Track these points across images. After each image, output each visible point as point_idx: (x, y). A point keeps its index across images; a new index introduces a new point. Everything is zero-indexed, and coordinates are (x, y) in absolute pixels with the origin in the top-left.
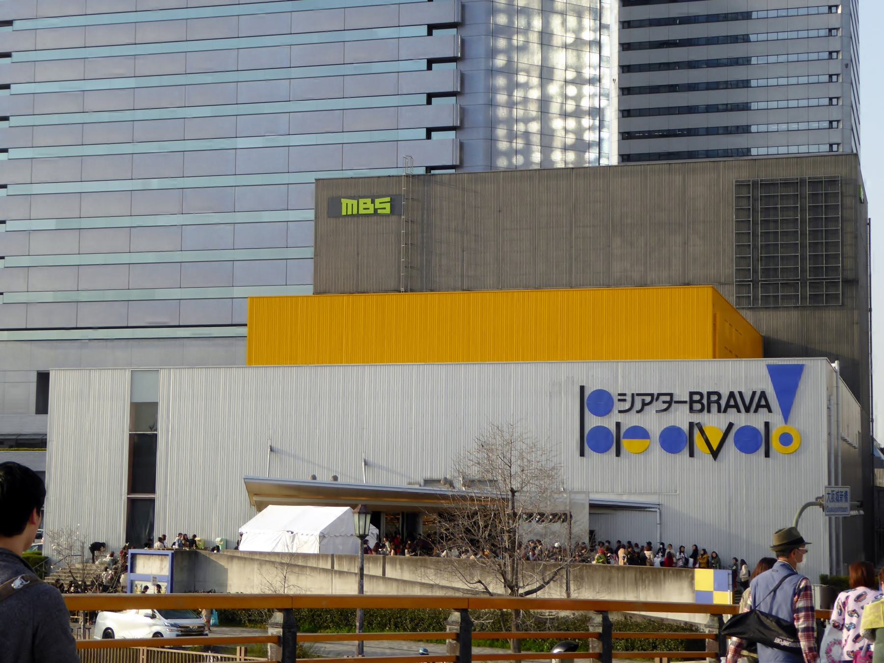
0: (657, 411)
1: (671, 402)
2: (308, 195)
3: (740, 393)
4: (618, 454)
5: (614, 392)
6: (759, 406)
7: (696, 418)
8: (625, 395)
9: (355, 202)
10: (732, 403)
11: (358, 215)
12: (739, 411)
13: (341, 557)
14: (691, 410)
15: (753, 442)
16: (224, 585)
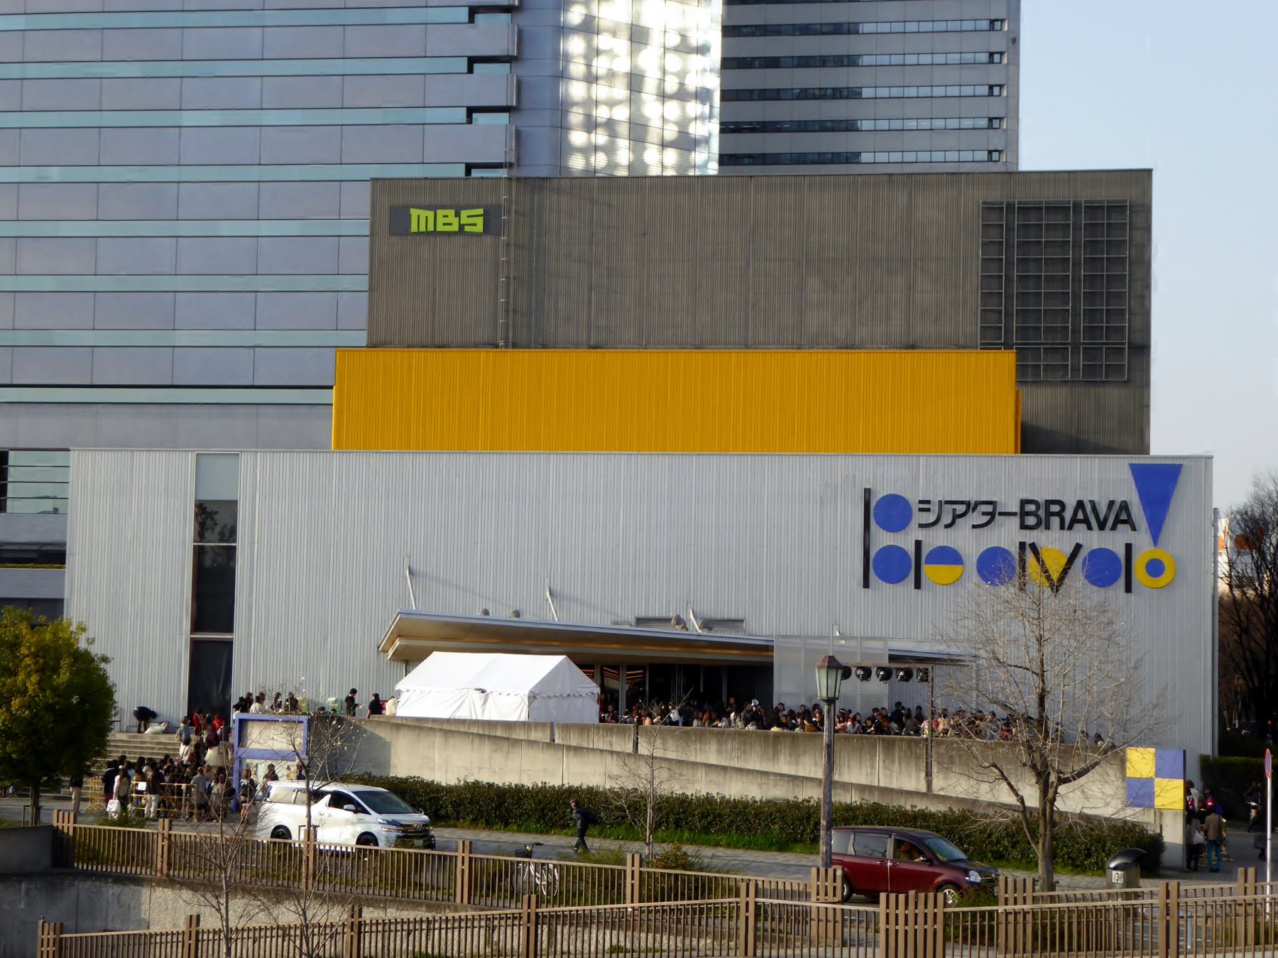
0: (974, 527)
1: (993, 513)
2: (360, 201)
3: (1093, 503)
4: (918, 585)
5: (913, 498)
6: (1117, 521)
7: (1029, 537)
8: (929, 502)
9: (430, 214)
10: (1080, 516)
11: (435, 233)
12: (1090, 528)
13: (566, 727)
14: (1023, 526)
15: (1111, 570)
16: (386, 764)
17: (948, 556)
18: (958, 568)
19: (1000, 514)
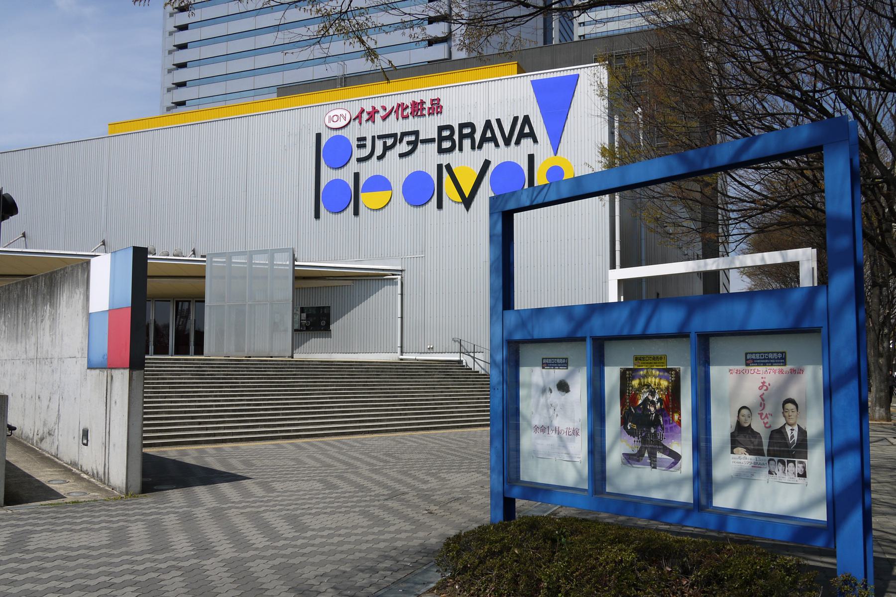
0: (402, 156)
1: (416, 141)
6: (522, 135)
7: (445, 159)
8: (364, 139)
10: (489, 134)
12: (497, 145)
14: (441, 151)
17: (380, 183)
18: (387, 194)
19: (425, 141)
